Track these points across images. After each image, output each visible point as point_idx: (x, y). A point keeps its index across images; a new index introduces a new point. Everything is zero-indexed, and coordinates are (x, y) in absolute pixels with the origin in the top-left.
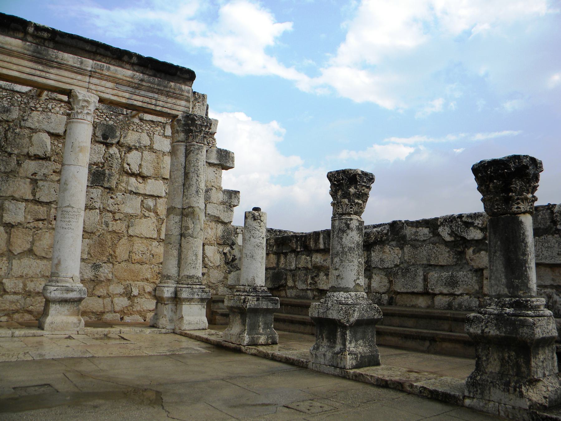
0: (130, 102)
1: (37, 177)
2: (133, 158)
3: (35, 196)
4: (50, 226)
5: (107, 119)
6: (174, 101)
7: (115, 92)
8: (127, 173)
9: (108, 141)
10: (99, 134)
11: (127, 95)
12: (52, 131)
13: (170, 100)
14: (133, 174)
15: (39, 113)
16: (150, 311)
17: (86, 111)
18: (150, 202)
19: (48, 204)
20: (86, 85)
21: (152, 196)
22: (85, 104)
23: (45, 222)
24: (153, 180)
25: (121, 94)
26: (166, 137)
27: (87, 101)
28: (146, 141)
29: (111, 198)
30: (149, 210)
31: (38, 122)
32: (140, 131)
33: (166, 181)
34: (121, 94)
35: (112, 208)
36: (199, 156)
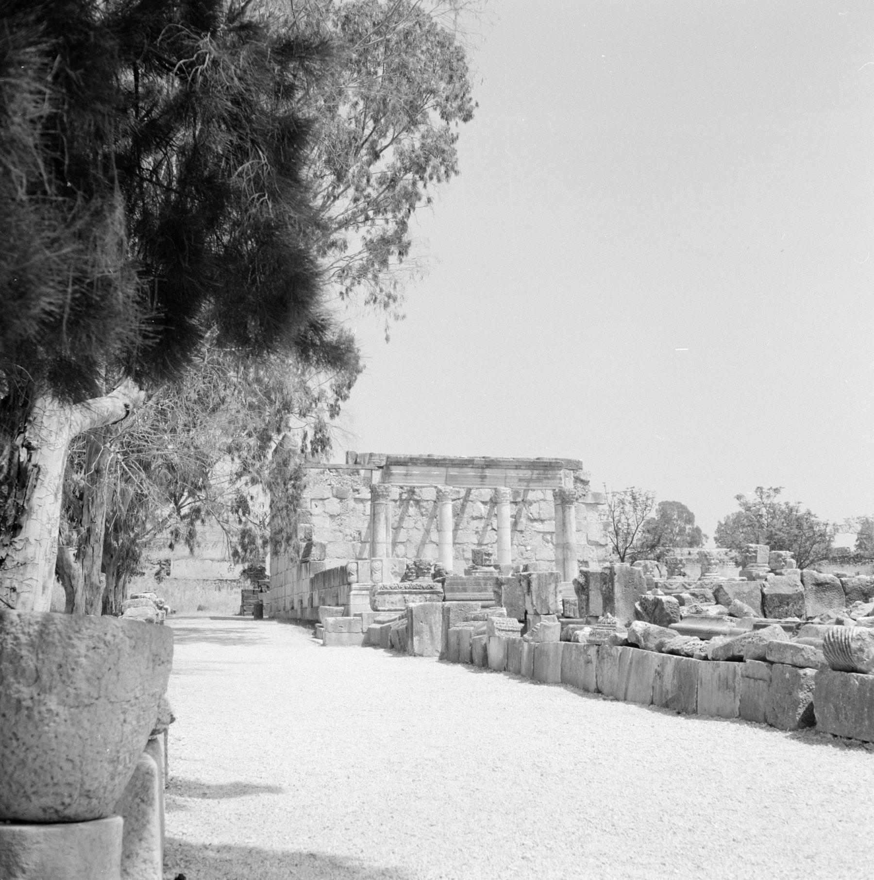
2: (534, 509)
14: (535, 520)
18: (549, 537)
21: (549, 533)
28: (541, 496)
30: (548, 542)
35: (524, 543)
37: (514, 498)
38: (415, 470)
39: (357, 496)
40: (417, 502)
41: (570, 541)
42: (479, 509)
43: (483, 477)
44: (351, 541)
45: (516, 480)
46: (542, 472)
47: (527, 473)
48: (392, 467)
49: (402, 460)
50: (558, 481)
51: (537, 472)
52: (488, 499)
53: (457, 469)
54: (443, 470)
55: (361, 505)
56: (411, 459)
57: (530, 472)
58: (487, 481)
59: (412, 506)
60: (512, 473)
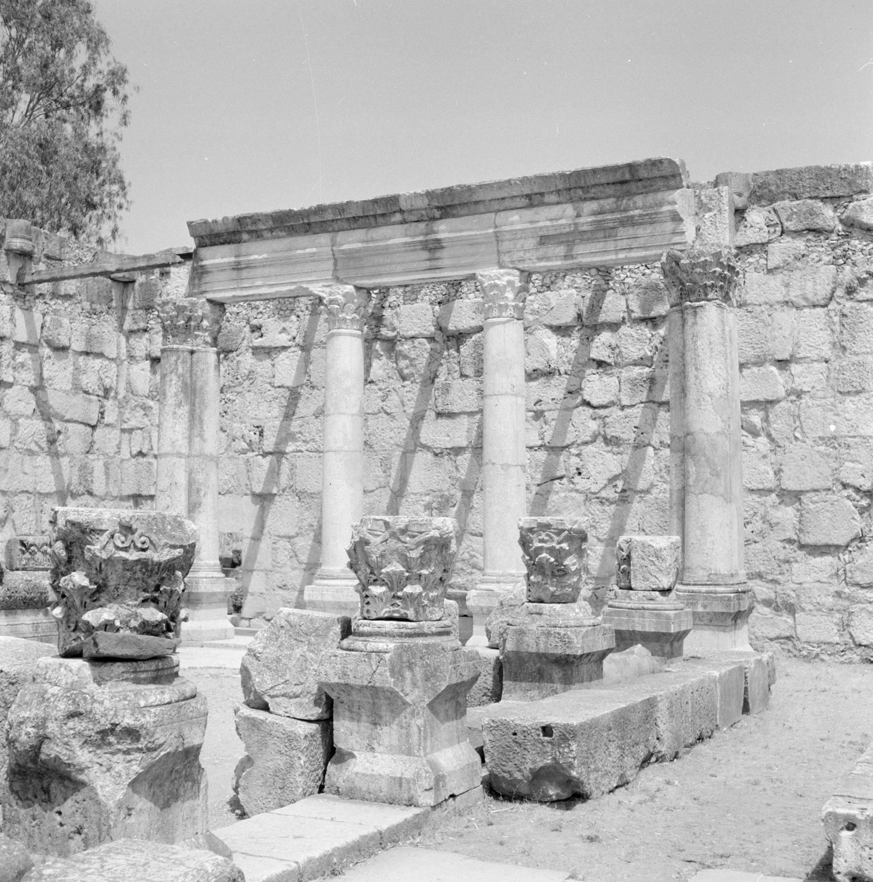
1: (543, 407)
3: (542, 439)
4: (572, 486)
5: (647, 271)
6: (649, 229)
9: (653, 314)
10: (635, 306)
12: (555, 323)
13: (640, 231)
16: (771, 640)
18: (756, 418)
23: (565, 480)
24: (755, 369)
30: (755, 434)
31: (533, 312)
36: (698, 328)
37: (646, 306)
38: (257, 252)
39: (258, 342)
40: (391, 343)
41: (695, 427)
42: (543, 347)
43: (433, 247)
44: (244, 452)
45: (531, 243)
46: (609, 203)
47: (559, 216)
48: (203, 252)
49: (220, 229)
50: (669, 226)
51: (594, 206)
52: (567, 317)
53: (360, 234)
54: (324, 239)
55: (267, 362)
56: (240, 220)
57: (569, 210)
58: (445, 257)
59: (379, 357)
60: (516, 220)
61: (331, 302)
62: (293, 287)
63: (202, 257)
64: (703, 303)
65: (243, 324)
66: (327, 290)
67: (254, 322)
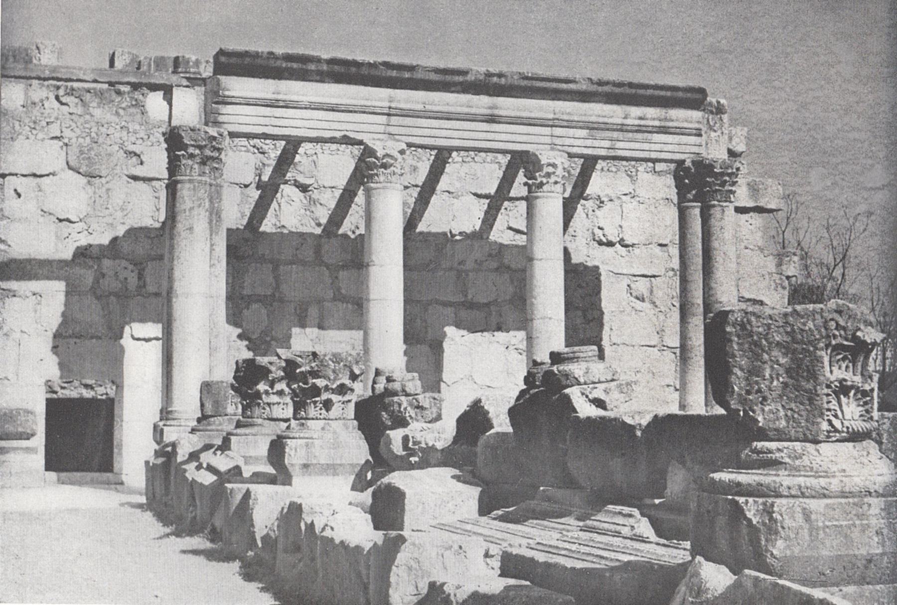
0: (612, 153)
3: (466, 296)
7: (589, 143)
8: (601, 243)
11: (607, 144)
15: (457, 165)
17: (553, 179)
19: (487, 305)
20: (548, 140)
22: (550, 169)
25: (596, 143)
26: (659, 173)
27: (554, 166)
29: (580, 286)
32: (614, 169)
33: (664, 248)
34: (596, 143)
61: (384, 156)
62: (338, 135)
63: (228, 87)
64: (727, 204)
65: (116, 148)
66: (378, 143)
67: (131, 148)
